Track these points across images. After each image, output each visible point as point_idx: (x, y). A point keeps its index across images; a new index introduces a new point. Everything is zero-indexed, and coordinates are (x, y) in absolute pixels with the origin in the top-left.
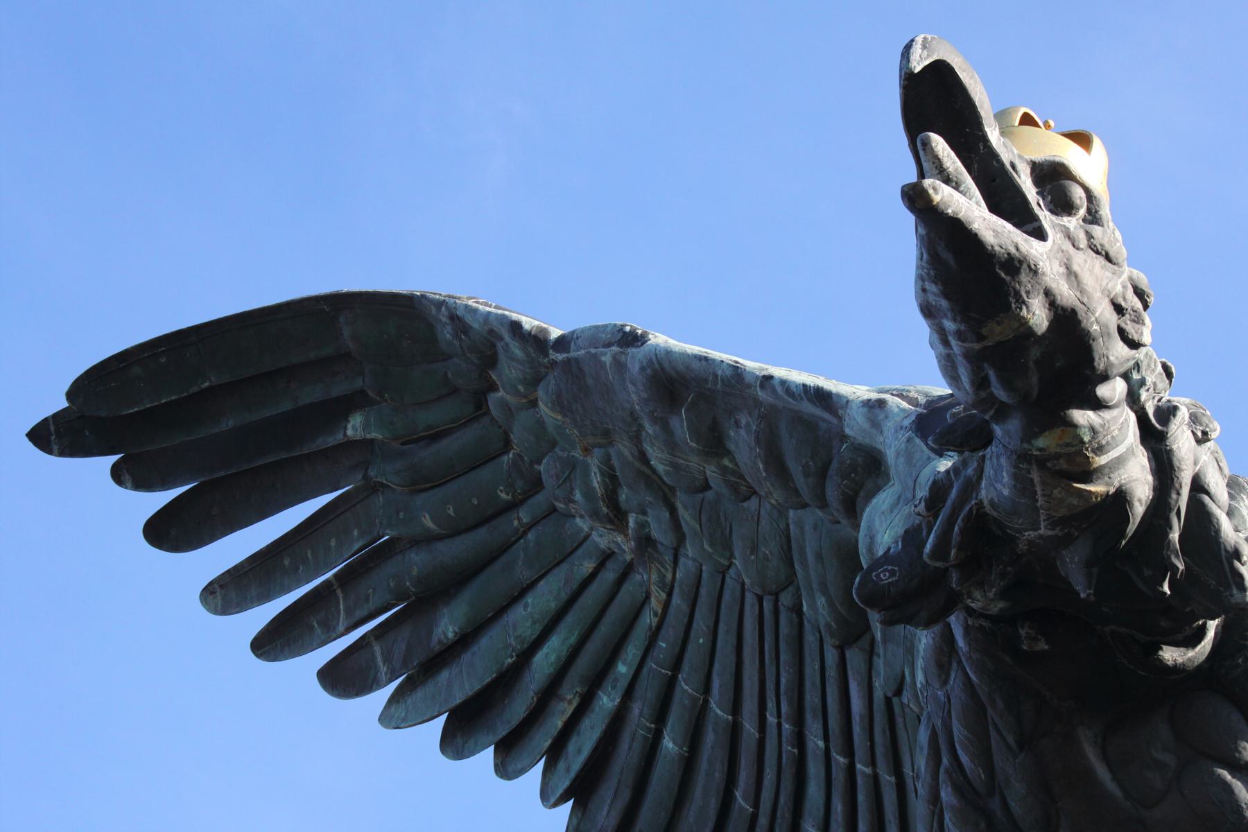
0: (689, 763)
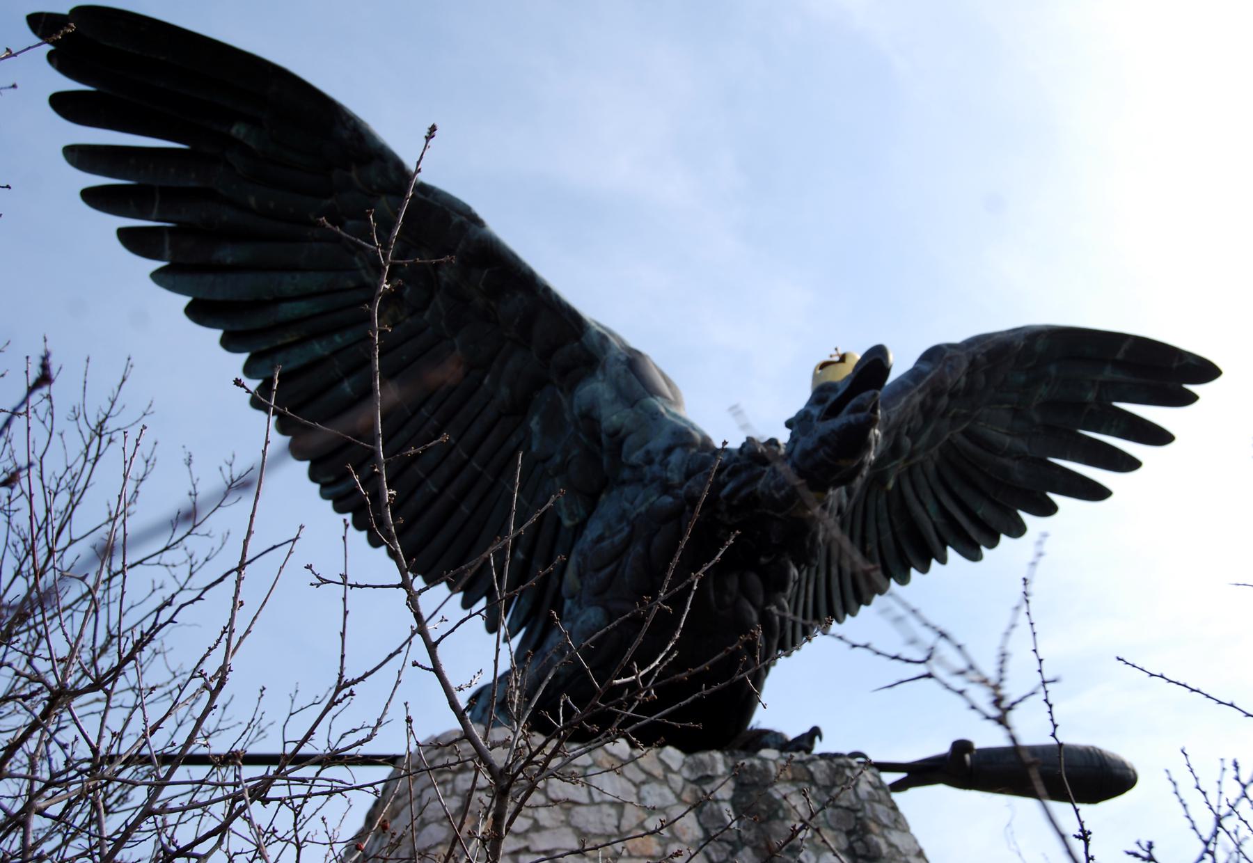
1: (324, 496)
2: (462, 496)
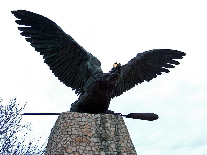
0: (57, 63)
1: (54, 75)
2: (72, 75)
